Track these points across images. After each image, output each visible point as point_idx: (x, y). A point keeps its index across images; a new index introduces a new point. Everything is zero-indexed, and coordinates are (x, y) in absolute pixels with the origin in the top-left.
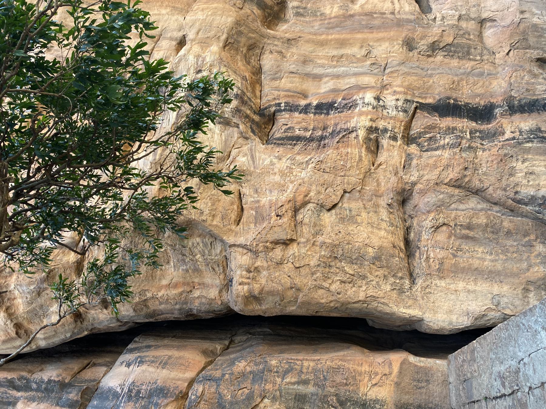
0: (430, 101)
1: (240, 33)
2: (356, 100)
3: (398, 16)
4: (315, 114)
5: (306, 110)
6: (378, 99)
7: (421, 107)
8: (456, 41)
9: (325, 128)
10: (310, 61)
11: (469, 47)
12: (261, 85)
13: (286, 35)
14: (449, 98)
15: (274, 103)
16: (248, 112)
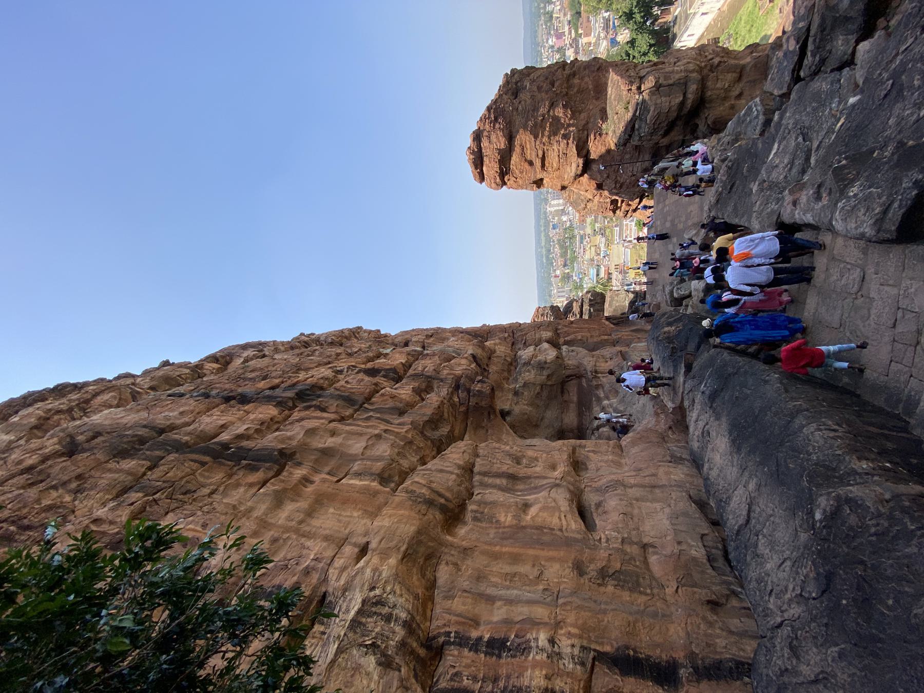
0: (607, 649)
1: (420, 542)
2: (529, 641)
3: (566, 534)
4: (486, 654)
5: (475, 646)
6: (552, 641)
7: (600, 657)
8: (623, 568)
9: (495, 680)
10: (484, 577)
11: (638, 576)
12: (433, 603)
13: (464, 543)
14: (627, 648)
15: (442, 631)
16: (415, 645)
